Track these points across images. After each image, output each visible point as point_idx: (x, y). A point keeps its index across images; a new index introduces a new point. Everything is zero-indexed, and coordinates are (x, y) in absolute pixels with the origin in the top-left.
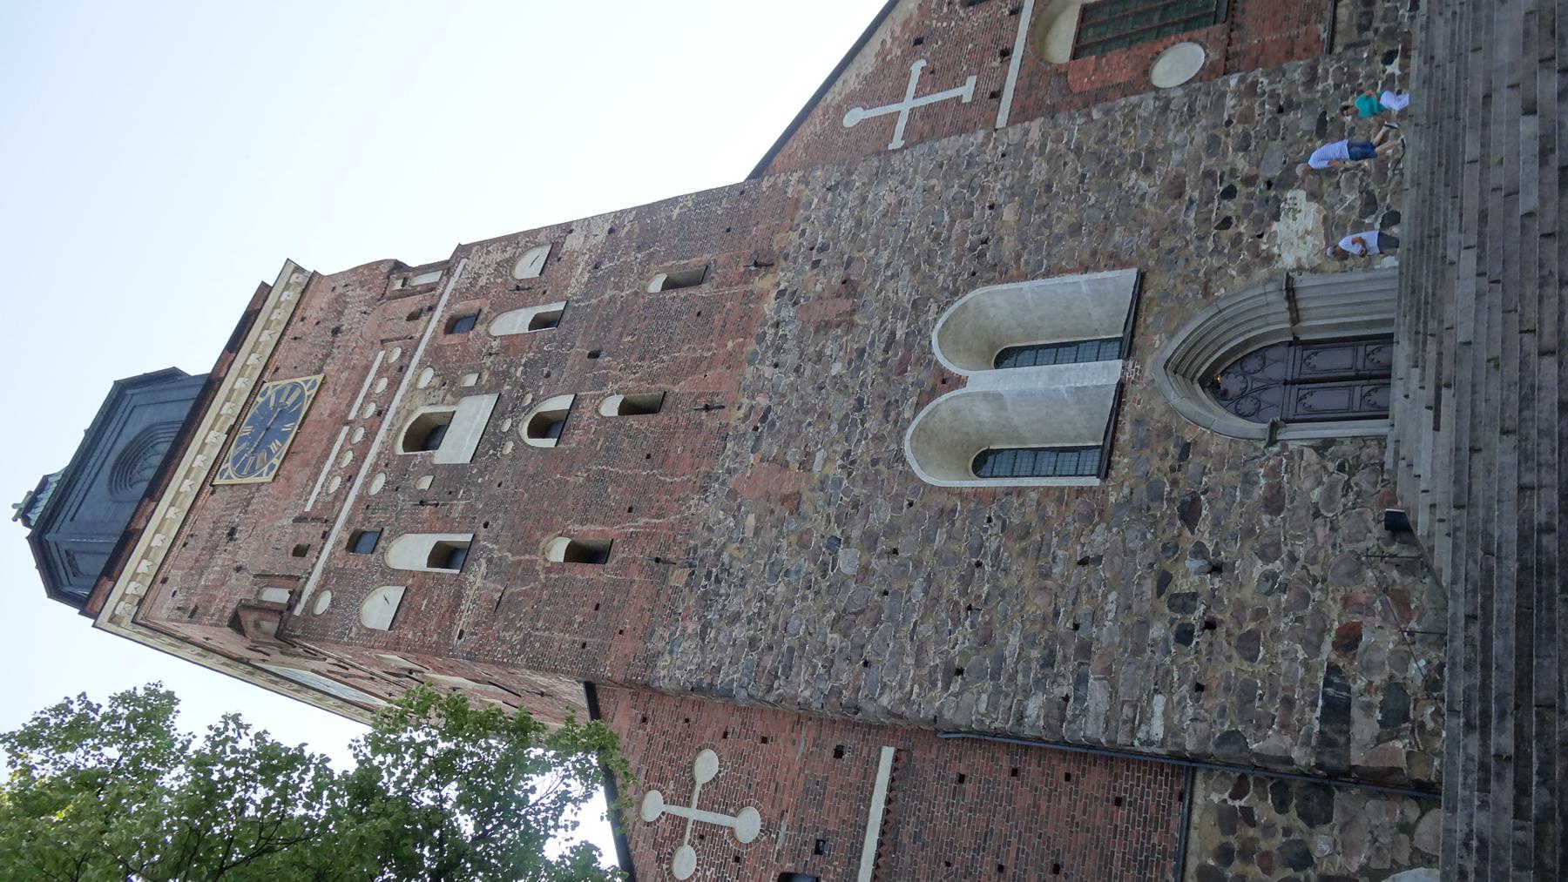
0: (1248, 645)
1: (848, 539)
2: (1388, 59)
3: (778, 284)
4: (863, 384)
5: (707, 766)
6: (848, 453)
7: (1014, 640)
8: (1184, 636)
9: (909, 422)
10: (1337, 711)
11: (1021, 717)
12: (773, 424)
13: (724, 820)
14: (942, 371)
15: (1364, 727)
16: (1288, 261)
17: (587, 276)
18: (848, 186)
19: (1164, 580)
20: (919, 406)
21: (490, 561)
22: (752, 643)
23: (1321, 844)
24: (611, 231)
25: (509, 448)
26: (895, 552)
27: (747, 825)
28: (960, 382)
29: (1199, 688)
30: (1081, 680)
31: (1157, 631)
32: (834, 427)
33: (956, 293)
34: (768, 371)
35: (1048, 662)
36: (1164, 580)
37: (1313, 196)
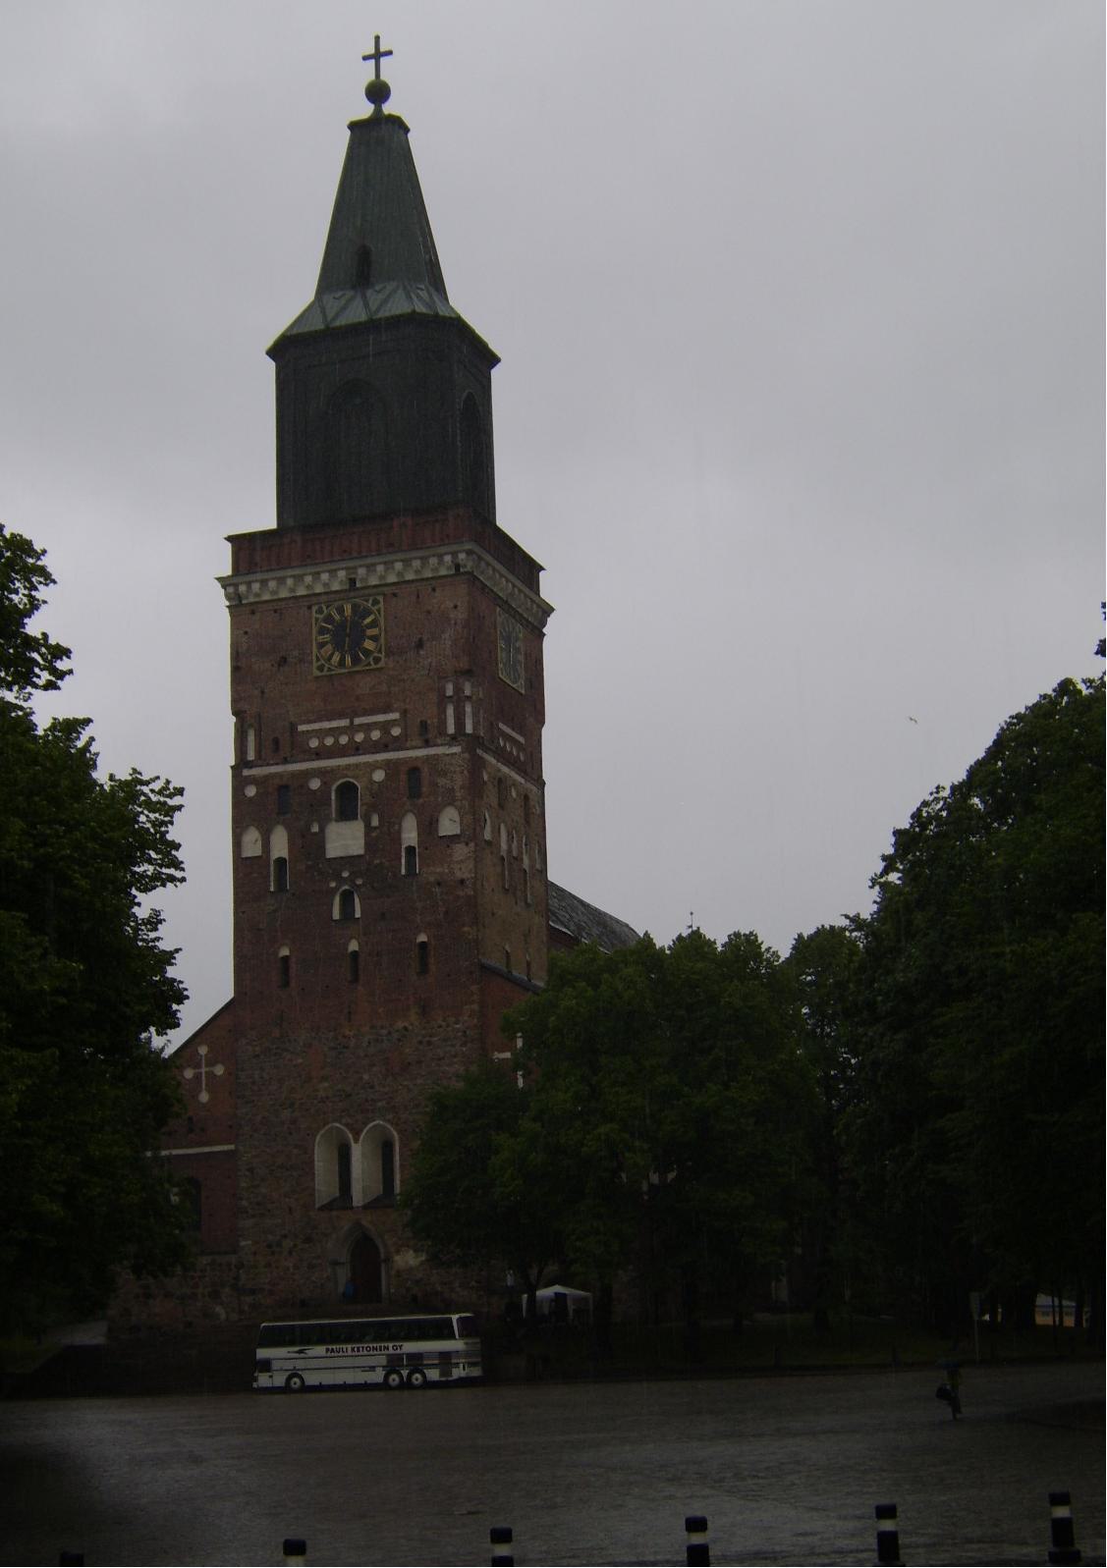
0: (268, 1265)
1: (293, 1111)
2: (476, 1282)
3: (412, 1024)
4: (358, 1094)
5: (219, 1070)
6: (327, 1098)
7: (264, 1190)
8: (269, 1246)
9: (341, 1123)
10: (253, 1292)
11: (241, 1199)
12: (340, 1053)
13: (204, 1086)
14: (362, 1131)
15: (249, 1299)
16: (397, 1258)
17: (432, 879)
18: (464, 1044)
19: (285, 1236)
20: (347, 1125)
21: (275, 911)
22: (254, 1083)
23: (227, 1290)
24: (462, 882)
25: (333, 885)
26: (291, 1134)
27: (204, 1097)
28: (356, 1141)
29: (255, 1254)
30: (253, 1216)
31: (270, 1237)
32: (340, 1086)
33: (397, 1125)
34: (366, 1039)
35: (258, 1204)
36: (285, 1236)
37: (422, 1263)
